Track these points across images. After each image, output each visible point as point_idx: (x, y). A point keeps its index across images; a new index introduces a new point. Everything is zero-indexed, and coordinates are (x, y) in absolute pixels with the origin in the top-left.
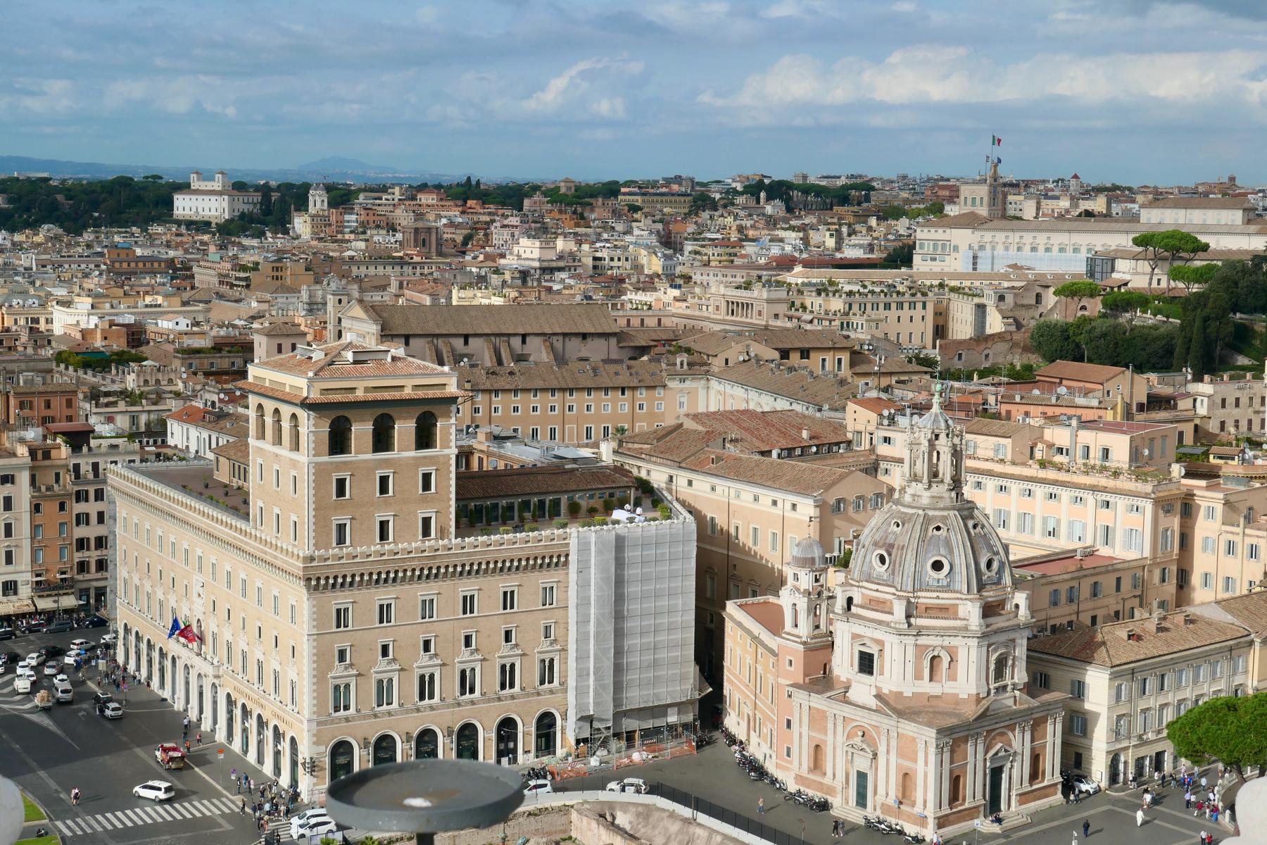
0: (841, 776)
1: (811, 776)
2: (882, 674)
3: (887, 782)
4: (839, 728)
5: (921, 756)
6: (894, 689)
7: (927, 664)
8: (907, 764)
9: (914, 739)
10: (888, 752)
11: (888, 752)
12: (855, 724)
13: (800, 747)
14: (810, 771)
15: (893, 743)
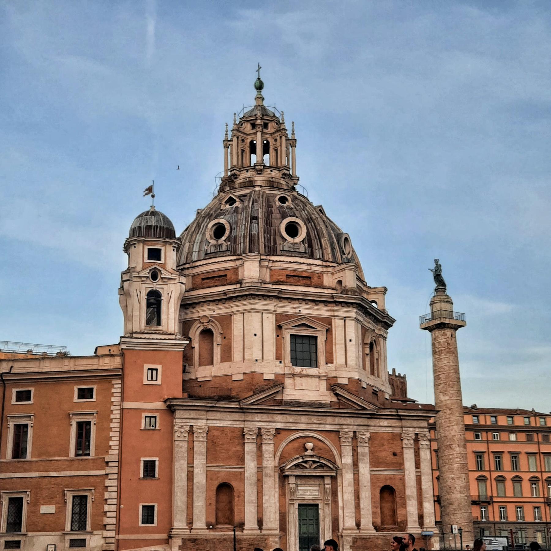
0: (272, 520)
1: (218, 534)
2: (329, 360)
3: (358, 506)
4: (268, 449)
5: (409, 456)
6: (356, 376)
7: (367, 350)
8: (387, 473)
9: (399, 437)
10: (355, 464)
11: (355, 464)
12: (292, 437)
13: (190, 493)
14: (210, 526)
15: (364, 450)
